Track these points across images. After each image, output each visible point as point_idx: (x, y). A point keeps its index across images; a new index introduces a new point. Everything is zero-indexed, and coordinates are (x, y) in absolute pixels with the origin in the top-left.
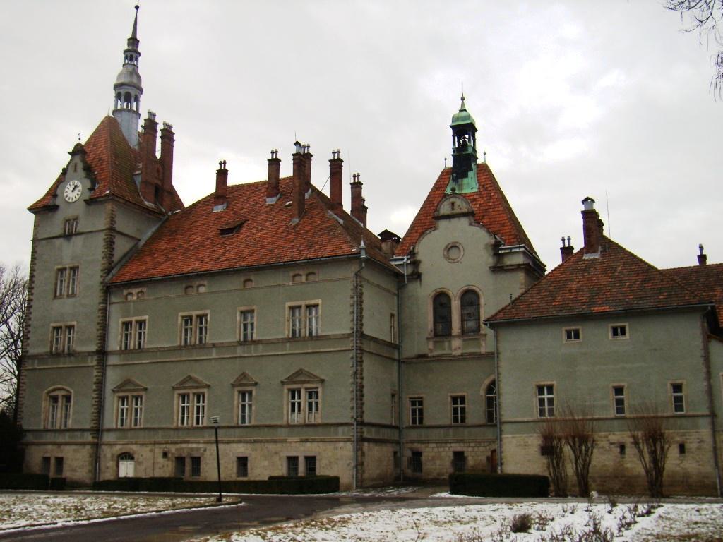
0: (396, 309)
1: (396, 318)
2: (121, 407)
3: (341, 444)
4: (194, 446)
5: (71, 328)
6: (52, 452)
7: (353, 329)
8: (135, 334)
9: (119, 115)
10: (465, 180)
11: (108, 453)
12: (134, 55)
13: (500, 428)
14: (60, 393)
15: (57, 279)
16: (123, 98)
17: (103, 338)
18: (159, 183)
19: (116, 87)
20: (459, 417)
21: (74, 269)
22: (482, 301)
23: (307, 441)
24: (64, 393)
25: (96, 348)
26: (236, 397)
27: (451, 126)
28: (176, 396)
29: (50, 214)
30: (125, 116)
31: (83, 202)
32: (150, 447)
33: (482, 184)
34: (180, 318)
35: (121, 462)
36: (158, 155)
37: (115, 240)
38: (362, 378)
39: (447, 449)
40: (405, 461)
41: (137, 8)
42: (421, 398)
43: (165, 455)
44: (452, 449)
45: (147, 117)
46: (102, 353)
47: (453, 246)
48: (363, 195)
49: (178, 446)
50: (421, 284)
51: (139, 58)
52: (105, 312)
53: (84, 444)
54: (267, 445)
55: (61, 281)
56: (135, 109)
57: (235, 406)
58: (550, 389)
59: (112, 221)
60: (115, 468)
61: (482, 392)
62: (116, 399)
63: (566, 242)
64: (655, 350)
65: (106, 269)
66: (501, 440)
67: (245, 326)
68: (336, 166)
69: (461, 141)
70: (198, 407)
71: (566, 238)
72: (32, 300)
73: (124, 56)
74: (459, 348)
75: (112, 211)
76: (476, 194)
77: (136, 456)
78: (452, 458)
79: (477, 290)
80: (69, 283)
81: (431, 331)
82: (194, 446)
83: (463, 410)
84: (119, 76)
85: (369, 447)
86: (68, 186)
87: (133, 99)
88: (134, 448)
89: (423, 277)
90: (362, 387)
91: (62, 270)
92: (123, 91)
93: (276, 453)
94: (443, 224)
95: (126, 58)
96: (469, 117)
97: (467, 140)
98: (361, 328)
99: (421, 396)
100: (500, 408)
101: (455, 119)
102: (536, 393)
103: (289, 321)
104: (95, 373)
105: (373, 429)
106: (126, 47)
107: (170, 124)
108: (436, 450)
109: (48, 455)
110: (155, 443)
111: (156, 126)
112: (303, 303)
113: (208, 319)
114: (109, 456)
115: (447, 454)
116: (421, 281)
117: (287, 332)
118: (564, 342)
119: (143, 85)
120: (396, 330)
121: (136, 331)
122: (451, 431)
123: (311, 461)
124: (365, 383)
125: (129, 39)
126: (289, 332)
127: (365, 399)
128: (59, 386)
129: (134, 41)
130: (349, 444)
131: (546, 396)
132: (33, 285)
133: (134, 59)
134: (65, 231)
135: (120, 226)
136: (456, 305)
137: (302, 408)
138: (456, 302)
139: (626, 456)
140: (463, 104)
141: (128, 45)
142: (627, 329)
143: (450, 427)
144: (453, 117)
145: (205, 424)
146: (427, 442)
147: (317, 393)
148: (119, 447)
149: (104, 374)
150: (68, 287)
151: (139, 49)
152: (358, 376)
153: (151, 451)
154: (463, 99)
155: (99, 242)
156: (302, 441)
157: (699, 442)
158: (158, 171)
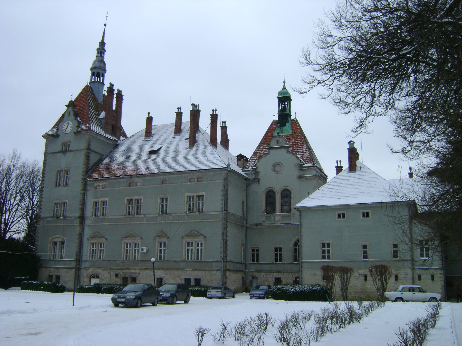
0: (245, 198)
1: (245, 203)
2: (92, 249)
3: (215, 272)
4: (133, 271)
5: (65, 204)
6: (54, 273)
7: (223, 209)
8: (101, 208)
9: (93, 85)
10: (285, 128)
11: (84, 273)
12: (102, 51)
13: (301, 265)
14: (58, 240)
15: (57, 176)
16: (95, 75)
17: (83, 210)
18: (114, 123)
19: (92, 69)
20: (278, 257)
21: (67, 172)
22: (292, 196)
23: (196, 270)
24: (61, 240)
25: (79, 215)
26: (157, 245)
27: (277, 97)
28: (123, 243)
29: (55, 139)
30: (96, 85)
31: (73, 133)
32: (108, 271)
33: (294, 130)
34: (126, 200)
35: (91, 279)
36: (114, 108)
37: (90, 155)
38: (227, 236)
39: (272, 276)
40: (248, 282)
41: (105, 25)
42: (258, 248)
43: (117, 275)
44: (274, 276)
45: (109, 86)
46: (82, 218)
47: (278, 164)
48: (227, 133)
49: (124, 271)
50: (259, 185)
51: (105, 53)
52: (84, 195)
54: (173, 272)
55: (60, 177)
56: (102, 82)
57: (156, 250)
58: (329, 245)
59: (89, 144)
60: (88, 282)
61: (292, 246)
62: (89, 244)
63: (339, 163)
64: (384, 225)
65: (85, 171)
66: (301, 272)
67: (163, 206)
68: (214, 118)
69: (283, 106)
70: (135, 250)
71: (339, 161)
72: (43, 187)
73: (97, 51)
74: (279, 221)
75: (90, 139)
76: (291, 135)
77: (100, 276)
78: (274, 281)
79: (290, 189)
80: (64, 178)
81: (264, 211)
82: (133, 271)
83: (281, 255)
84: (94, 62)
85: (229, 274)
86: (65, 124)
87: (101, 76)
88: (99, 271)
89: (260, 181)
90: (226, 241)
91: (60, 172)
92: (96, 71)
93: (179, 276)
94: (272, 152)
95: (98, 53)
96: (287, 93)
97: (286, 105)
98: (227, 209)
99: (258, 247)
100: (301, 254)
101: (280, 93)
102: (321, 247)
103: (187, 203)
104: (78, 229)
105: (232, 264)
106: (98, 47)
107: (121, 90)
108: (265, 276)
109: (51, 274)
110: (111, 269)
111: (114, 92)
112: (195, 194)
113: (142, 201)
114: (85, 275)
115: (271, 278)
116: (259, 183)
117: (186, 210)
118: (337, 219)
119: (107, 68)
120: (245, 210)
121: (101, 206)
122: (274, 266)
123: (198, 281)
124: (228, 239)
125: (100, 43)
126: (187, 210)
127: (228, 248)
128: (58, 236)
129: (102, 44)
130: (219, 272)
131: (326, 249)
132: (44, 179)
133: (102, 53)
134: (62, 149)
135: (93, 148)
136: (278, 197)
137: (193, 252)
138: (278, 195)
139: (368, 281)
140: (284, 85)
141: (99, 46)
142: (370, 213)
143: (273, 264)
144: (279, 92)
145: (139, 259)
146: (261, 271)
147: (202, 244)
149: (83, 230)
150: (64, 181)
151: (105, 48)
152: (225, 234)
153: (109, 273)
154: (284, 82)
155: (81, 157)
156: (193, 270)
157: (405, 274)
158: (114, 117)
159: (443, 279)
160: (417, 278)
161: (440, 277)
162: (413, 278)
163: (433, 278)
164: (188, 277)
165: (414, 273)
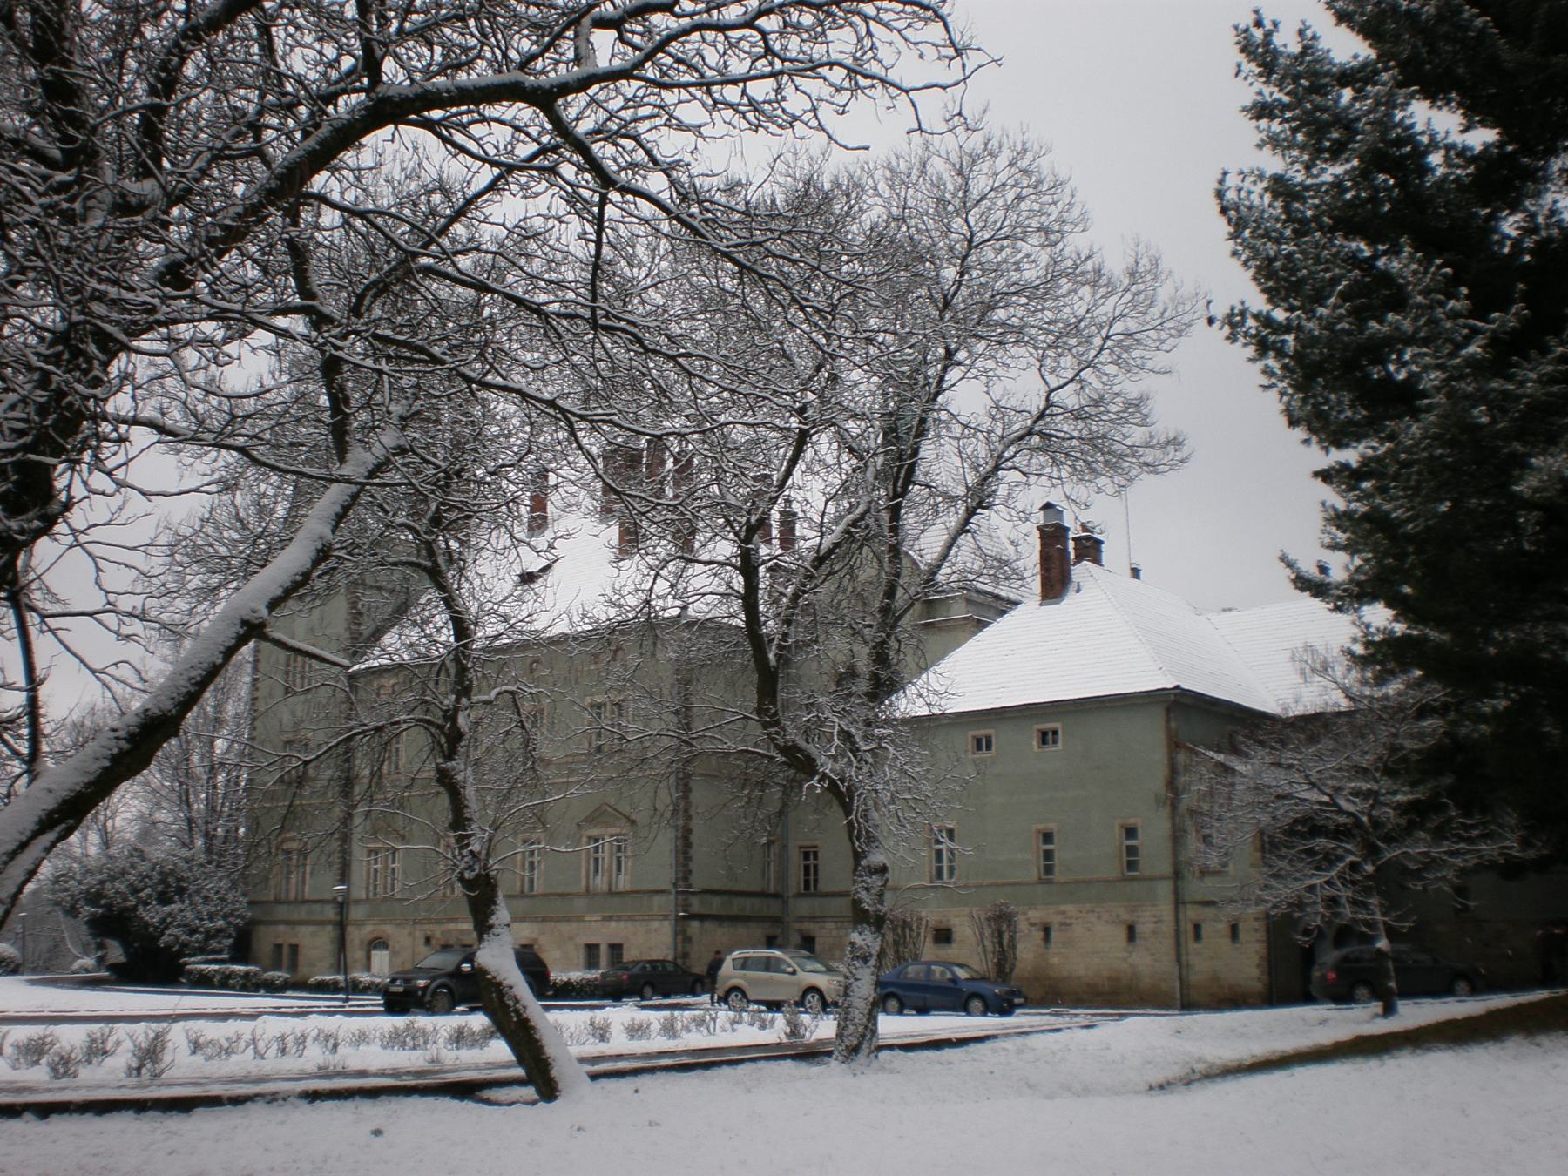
23: (610, 918)
38: (689, 818)
43: (428, 940)
53: (321, 923)
54: (558, 924)
77: (391, 943)
88: (388, 929)
90: (689, 831)
93: (571, 939)
108: (834, 933)
109: (279, 941)
114: (357, 942)
130: (666, 923)
139: (1053, 945)
148: (369, 928)
157: (1156, 922)
159: (1262, 935)
160: (1191, 934)
161: (1256, 930)
162: (1177, 932)
163: (1234, 931)
164: (592, 940)
165: (1181, 916)
